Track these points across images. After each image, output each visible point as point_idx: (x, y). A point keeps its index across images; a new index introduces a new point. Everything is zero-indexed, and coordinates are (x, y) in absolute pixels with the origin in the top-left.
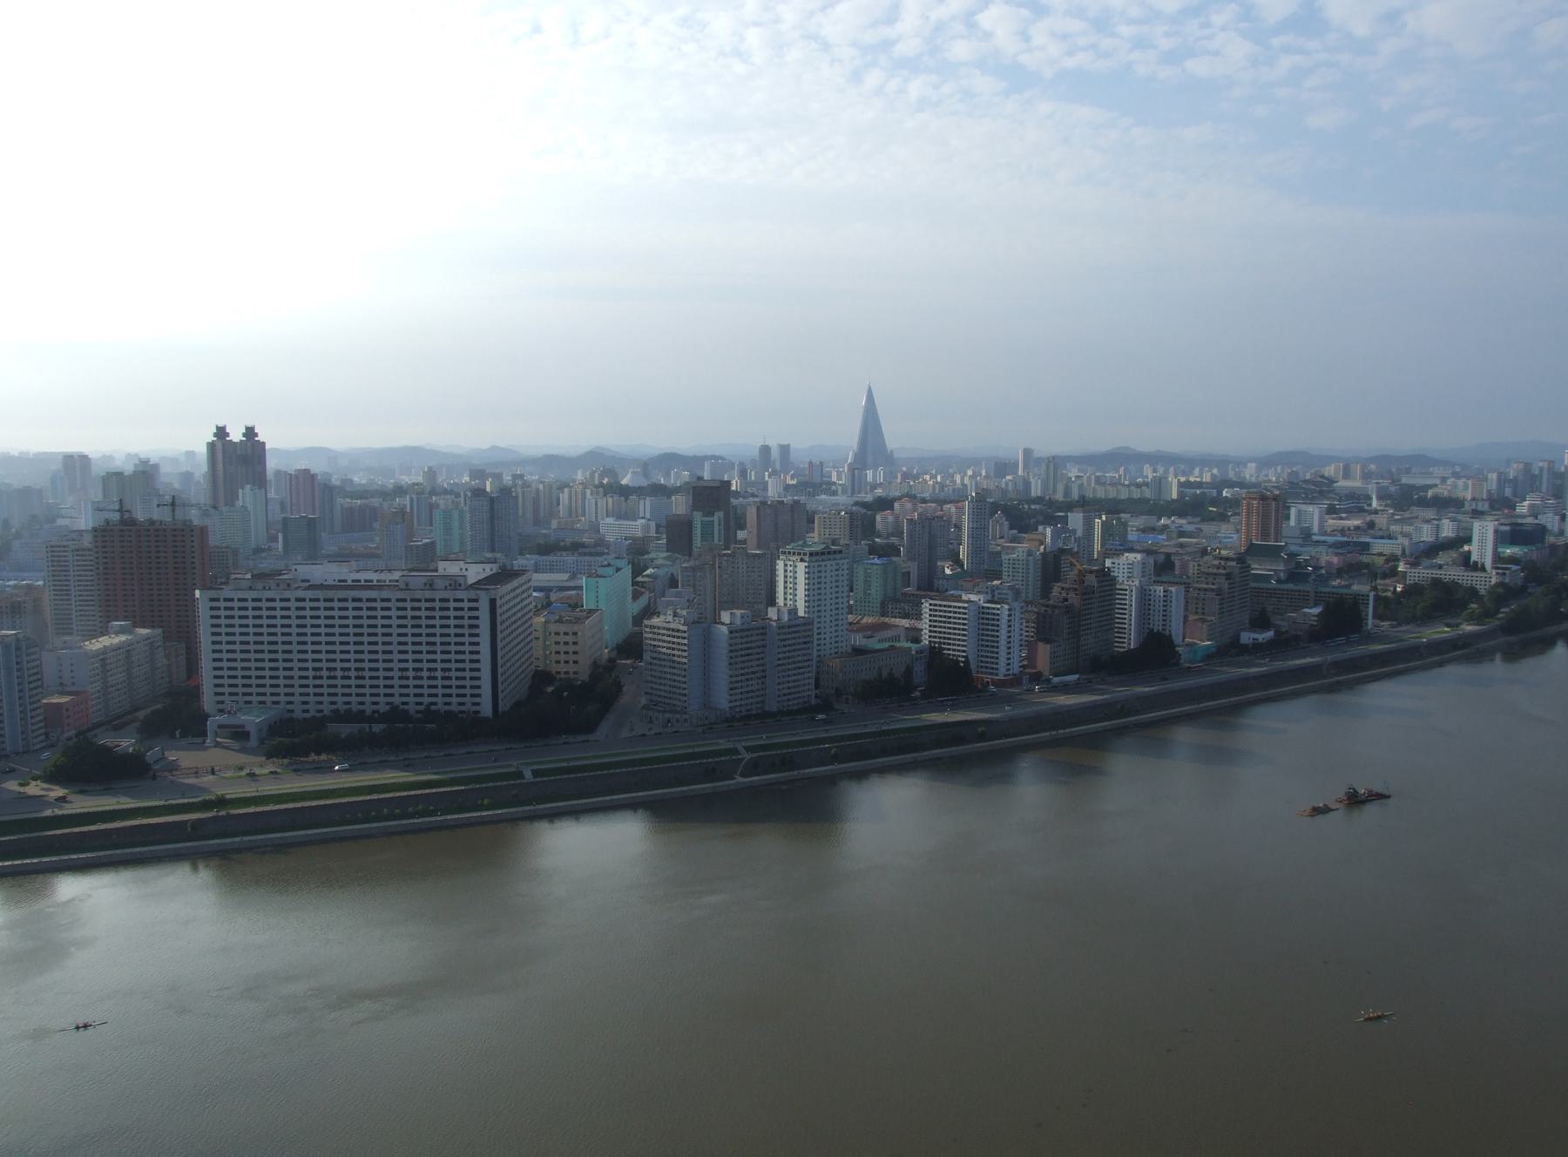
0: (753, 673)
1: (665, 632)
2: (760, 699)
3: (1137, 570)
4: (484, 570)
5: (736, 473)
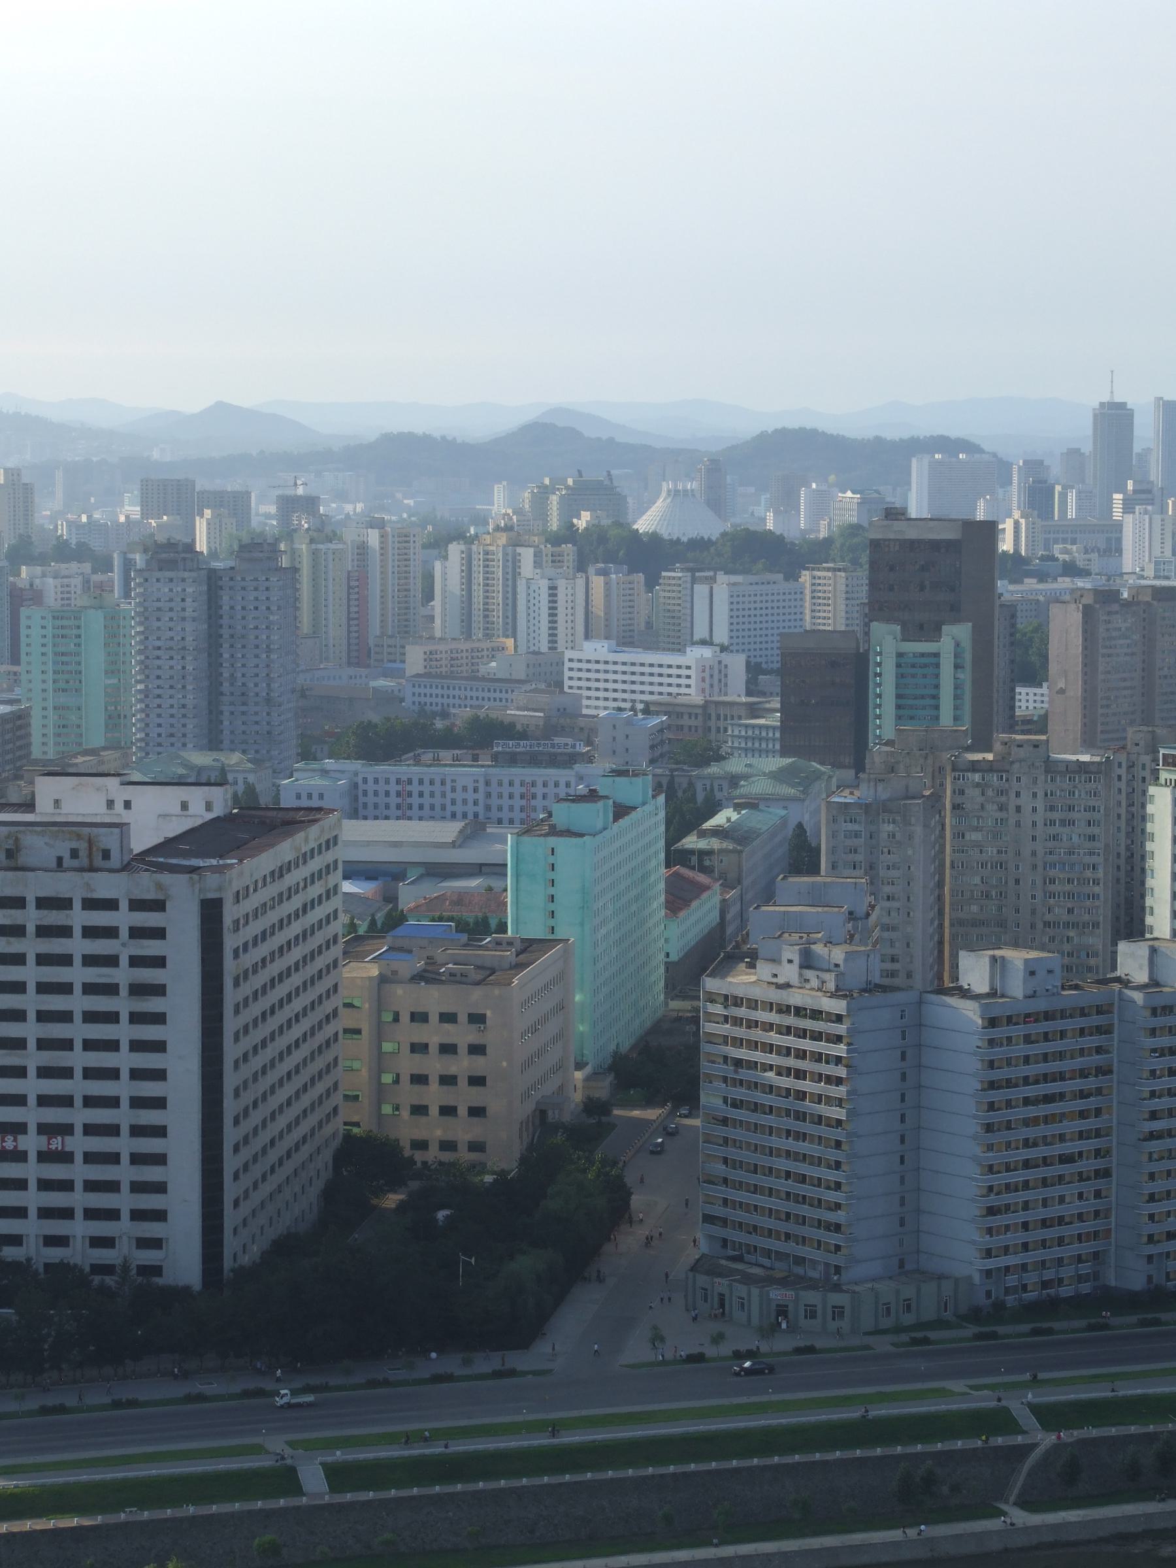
0: (1065, 1159)
1: (773, 1017)
2: (1086, 1248)
4: (184, 806)
5: (1015, 493)
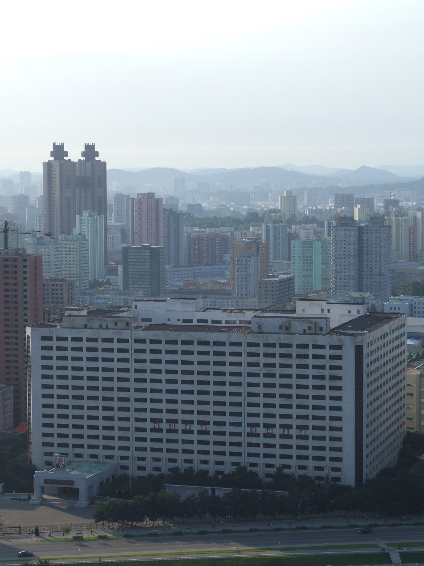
4: (349, 312)
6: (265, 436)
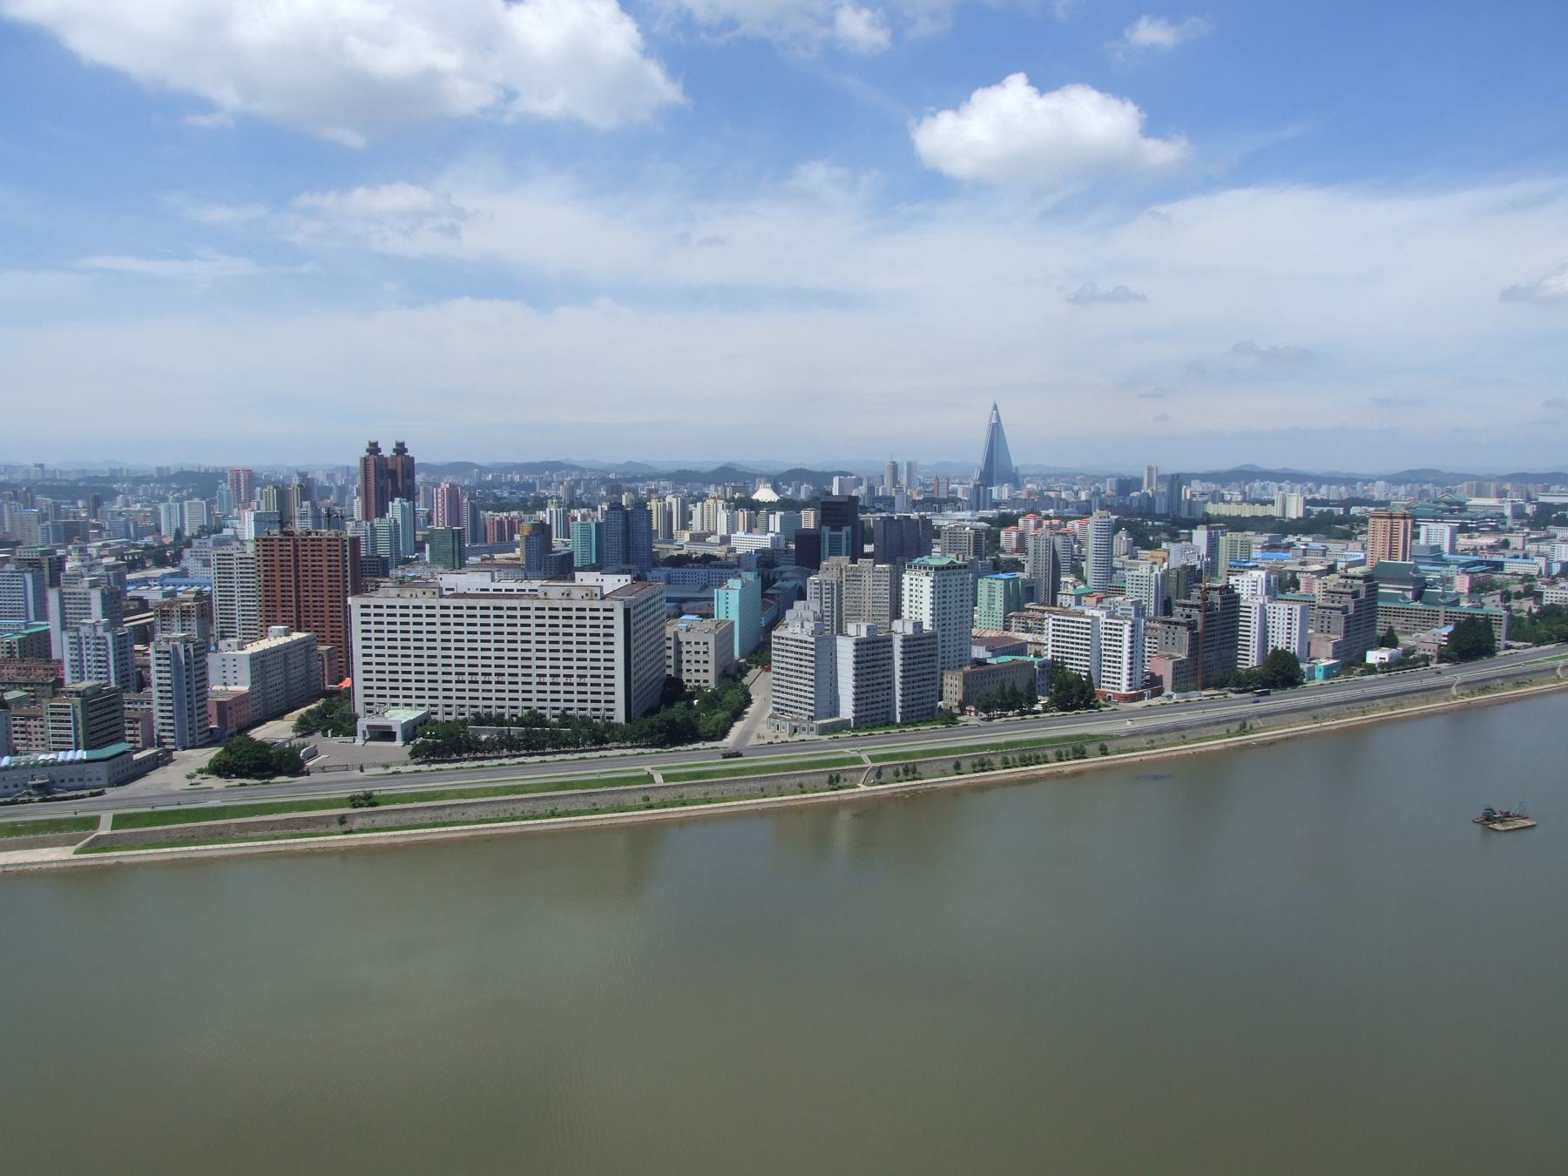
0: (879, 684)
3: (1261, 589)
4: (619, 581)
6: (552, 684)
